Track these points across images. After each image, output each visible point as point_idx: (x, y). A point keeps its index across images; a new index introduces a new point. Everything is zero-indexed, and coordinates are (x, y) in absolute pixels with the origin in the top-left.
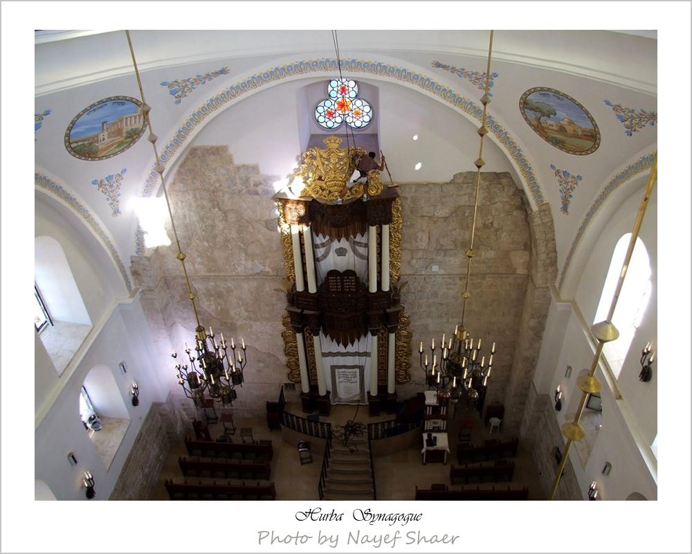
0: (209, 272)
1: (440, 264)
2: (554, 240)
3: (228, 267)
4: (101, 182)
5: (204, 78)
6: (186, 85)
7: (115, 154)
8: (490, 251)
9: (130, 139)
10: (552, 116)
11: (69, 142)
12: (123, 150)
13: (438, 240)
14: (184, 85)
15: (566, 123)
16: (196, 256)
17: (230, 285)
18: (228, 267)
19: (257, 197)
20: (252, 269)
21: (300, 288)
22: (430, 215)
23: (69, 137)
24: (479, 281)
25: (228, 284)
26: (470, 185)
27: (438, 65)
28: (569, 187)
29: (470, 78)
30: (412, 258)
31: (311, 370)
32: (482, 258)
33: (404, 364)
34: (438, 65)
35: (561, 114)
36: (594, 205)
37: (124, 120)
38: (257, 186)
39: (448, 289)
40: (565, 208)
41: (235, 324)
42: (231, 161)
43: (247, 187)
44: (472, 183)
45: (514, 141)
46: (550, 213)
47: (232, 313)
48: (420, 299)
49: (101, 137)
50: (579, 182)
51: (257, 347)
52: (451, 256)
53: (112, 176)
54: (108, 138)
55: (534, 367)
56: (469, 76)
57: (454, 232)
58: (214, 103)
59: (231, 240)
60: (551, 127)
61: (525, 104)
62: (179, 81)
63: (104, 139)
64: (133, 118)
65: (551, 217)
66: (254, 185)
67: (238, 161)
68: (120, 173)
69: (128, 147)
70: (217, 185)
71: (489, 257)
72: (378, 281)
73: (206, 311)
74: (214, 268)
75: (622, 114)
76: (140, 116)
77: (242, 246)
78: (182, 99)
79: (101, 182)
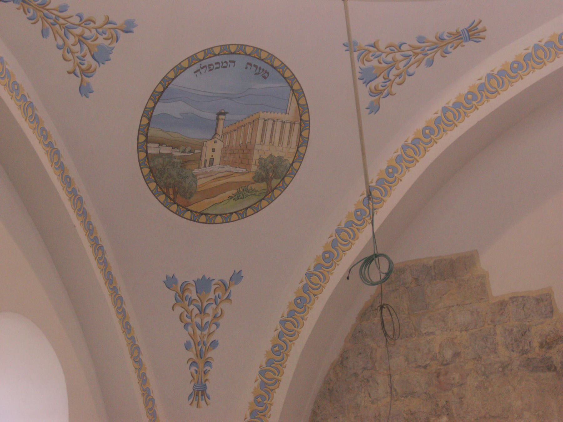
4: (184, 288)
5: (434, 48)
6: (395, 61)
7: (227, 218)
9: (263, 185)
11: (146, 136)
12: (242, 214)
14: (389, 58)
19: (550, 374)
23: (150, 119)
37: (261, 122)
38: (550, 348)
42: (483, 288)
43: (524, 352)
49: (207, 154)
53: (210, 281)
54: (223, 162)
58: (450, 115)
62: (382, 46)
63: (211, 164)
64: (278, 125)
66: (541, 346)
67: (499, 289)
68: (227, 281)
69: (256, 208)
70: (448, 354)
76: (292, 124)
78: (382, 101)
79: (184, 288)
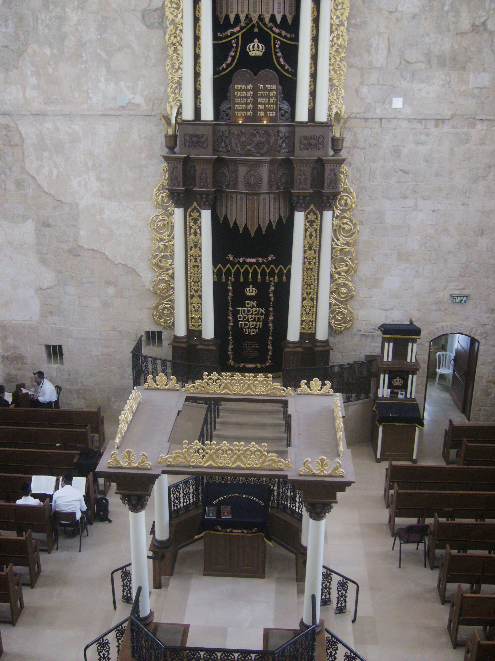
0: (45, 104)
3: (76, 95)
8: (482, 74)
16: (29, 73)
17: (77, 127)
18: (76, 95)
20: (115, 99)
21: (188, 114)
24: (465, 130)
25: (73, 126)
30: (362, 83)
31: (192, 296)
32: (471, 86)
33: (344, 290)
39: (418, 143)
41: (77, 205)
47: (74, 183)
48: (373, 162)
51: (108, 254)
52: (422, 81)
57: (427, 39)
59: (88, 45)
71: (480, 86)
72: (309, 110)
73: (33, 178)
74: (55, 97)
77: (103, 55)
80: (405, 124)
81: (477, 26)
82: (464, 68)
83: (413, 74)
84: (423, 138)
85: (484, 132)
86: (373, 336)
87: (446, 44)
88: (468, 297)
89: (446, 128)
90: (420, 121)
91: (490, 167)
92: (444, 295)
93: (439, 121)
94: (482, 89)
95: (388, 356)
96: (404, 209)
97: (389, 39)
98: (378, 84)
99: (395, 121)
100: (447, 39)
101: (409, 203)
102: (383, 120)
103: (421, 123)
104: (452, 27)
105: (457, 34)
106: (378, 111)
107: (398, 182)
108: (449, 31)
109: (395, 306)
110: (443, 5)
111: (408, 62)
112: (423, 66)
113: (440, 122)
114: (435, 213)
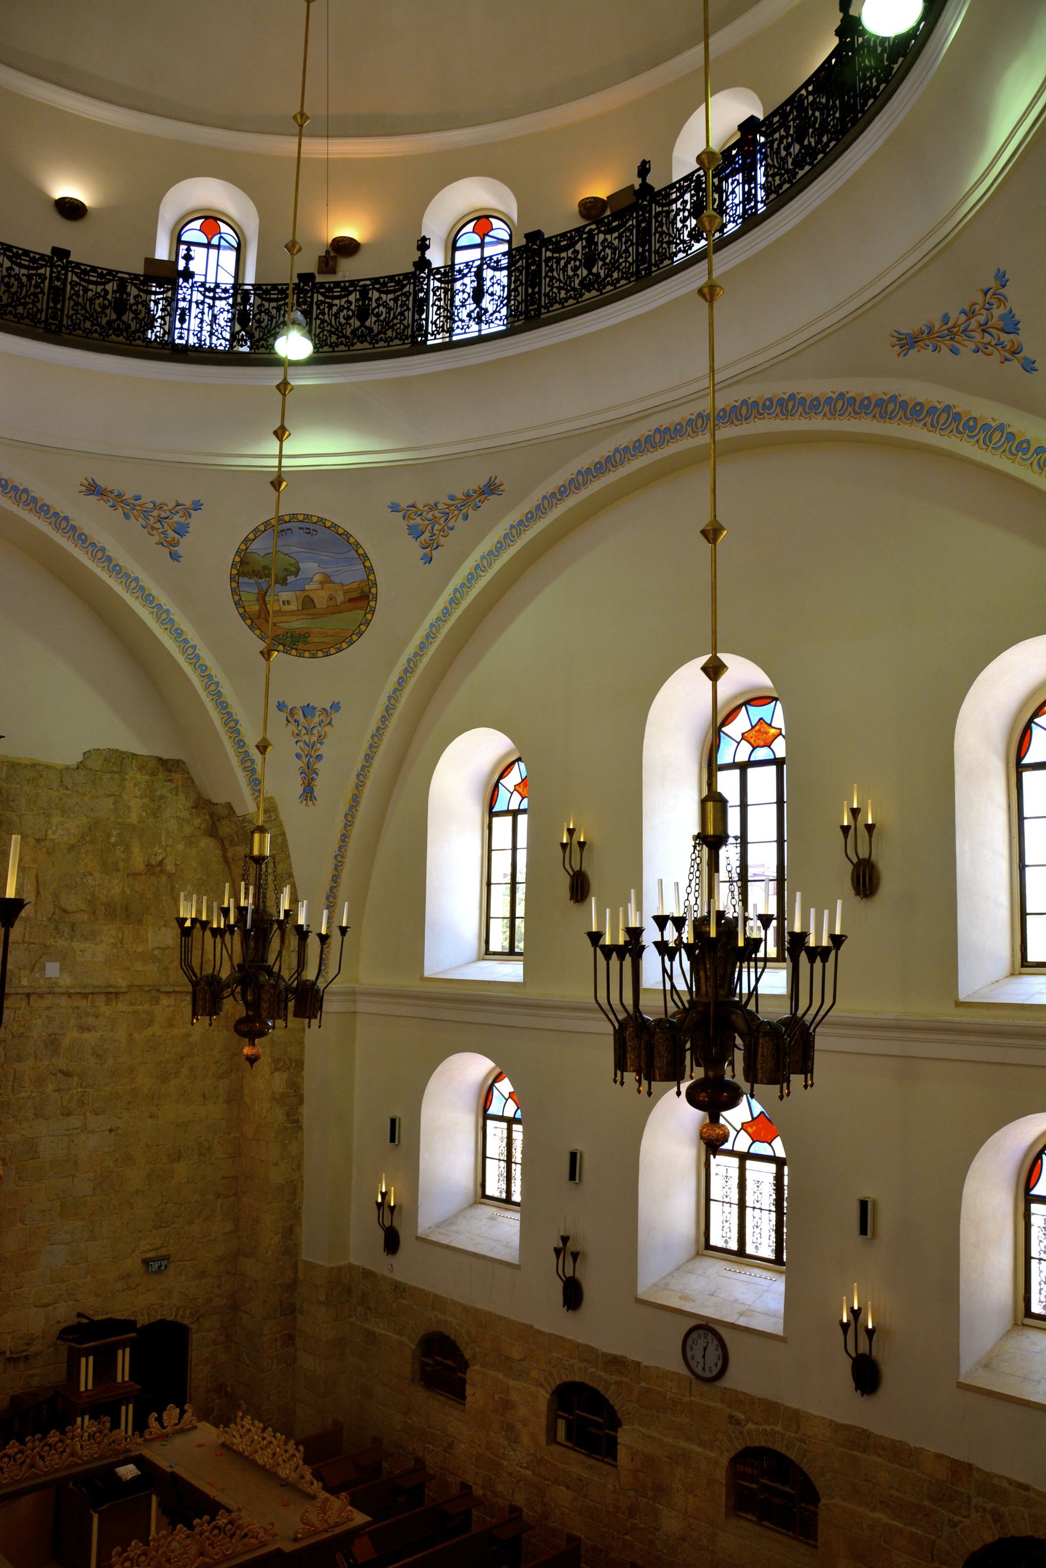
1: (63, 958)
2: (291, 875)
8: (164, 930)
10: (291, 579)
13: (56, 896)
15: (317, 586)
22: (39, 836)
24: (147, 1007)
26: (116, 776)
27: (93, 489)
28: (314, 739)
29: (146, 518)
32: (150, 945)
34: (93, 489)
35: (309, 567)
36: (367, 755)
39: (83, 1029)
40: (308, 793)
44: (118, 773)
45: (207, 663)
46: (277, 816)
48: (19, 1059)
50: (335, 717)
52: (86, 939)
55: (297, 1214)
56: (146, 514)
57: (90, 879)
60: (286, 608)
61: (245, 568)
65: (281, 825)
71: (162, 945)
75: (418, 520)
80: (63, 1001)
81: (152, 866)
82: (140, 921)
83: (73, 927)
84: (91, 1021)
85: (172, 1009)
86: (27, 1357)
87: (116, 888)
88: (166, 1258)
89: (122, 1006)
90: (85, 996)
91: (182, 1058)
92: (133, 1263)
93: (112, 995)
94: (164, 949)
95: (86, 1380)
96: (67, 1133)
97: (37, 876)
98: (24, 942)
99: (50, 997)
100: (117, 881)
101: (75, 1121)
102: (32, 997)
103: (87, 998)
104: (121, 865)
105: (128, 875)
106: (25, 982)
107: (58, 1090)
108: (118, 870)
109: (60, 1295)
110: (109, 836)
111: (65, 911)
112: (86, 916)
113: (113, 996)
114: (113, 1133)
